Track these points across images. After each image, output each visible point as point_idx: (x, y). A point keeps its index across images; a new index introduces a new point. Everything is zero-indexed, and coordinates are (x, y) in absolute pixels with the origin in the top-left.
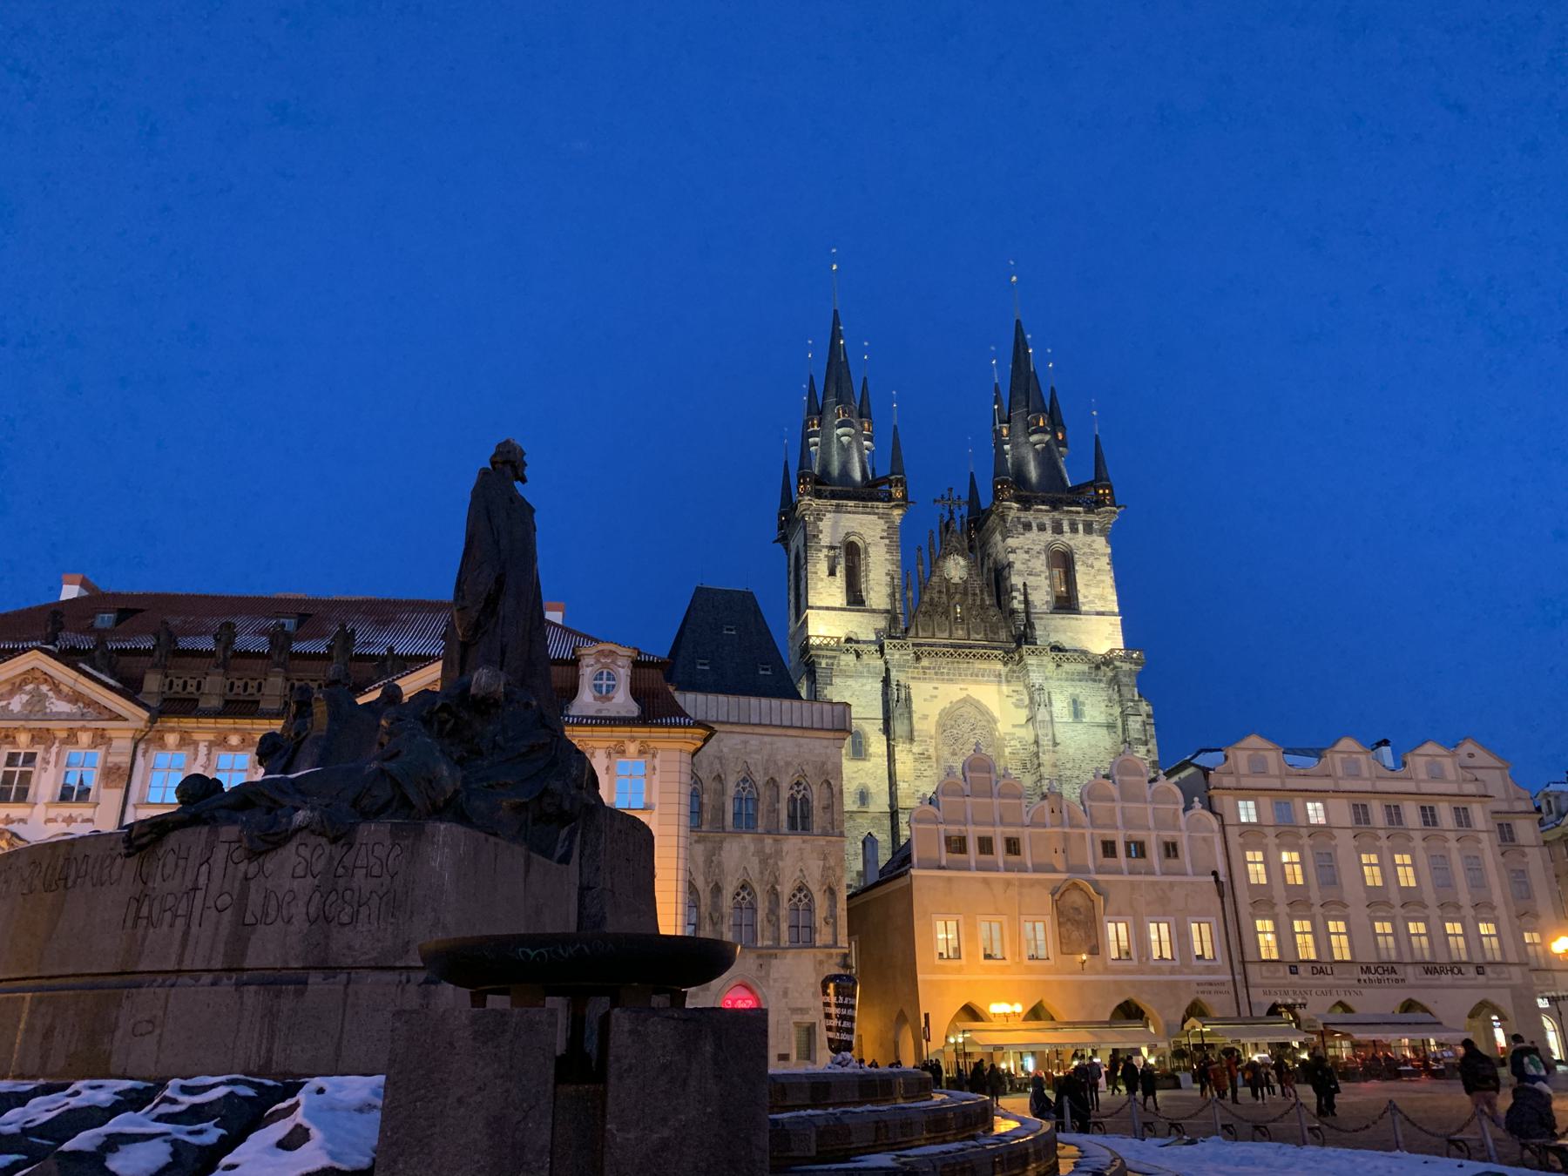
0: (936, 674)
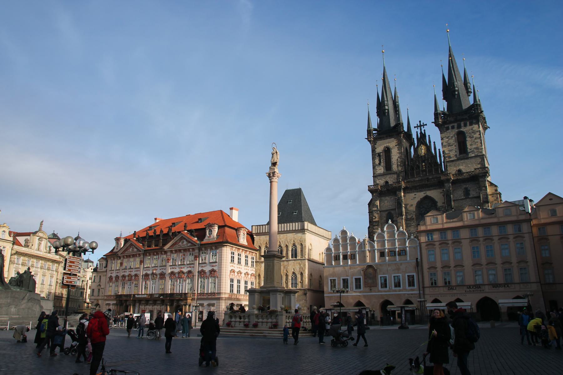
0: (415, 190)
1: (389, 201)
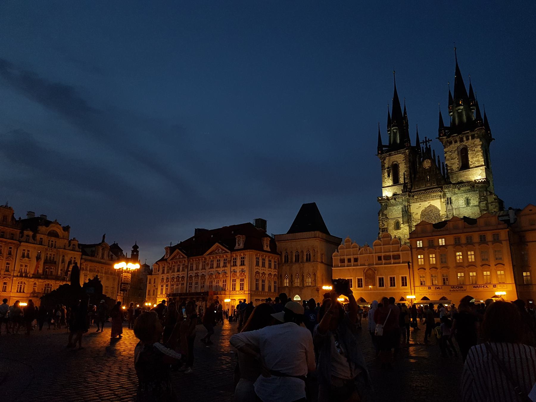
0: (420, 200)
1: (397, 210)
